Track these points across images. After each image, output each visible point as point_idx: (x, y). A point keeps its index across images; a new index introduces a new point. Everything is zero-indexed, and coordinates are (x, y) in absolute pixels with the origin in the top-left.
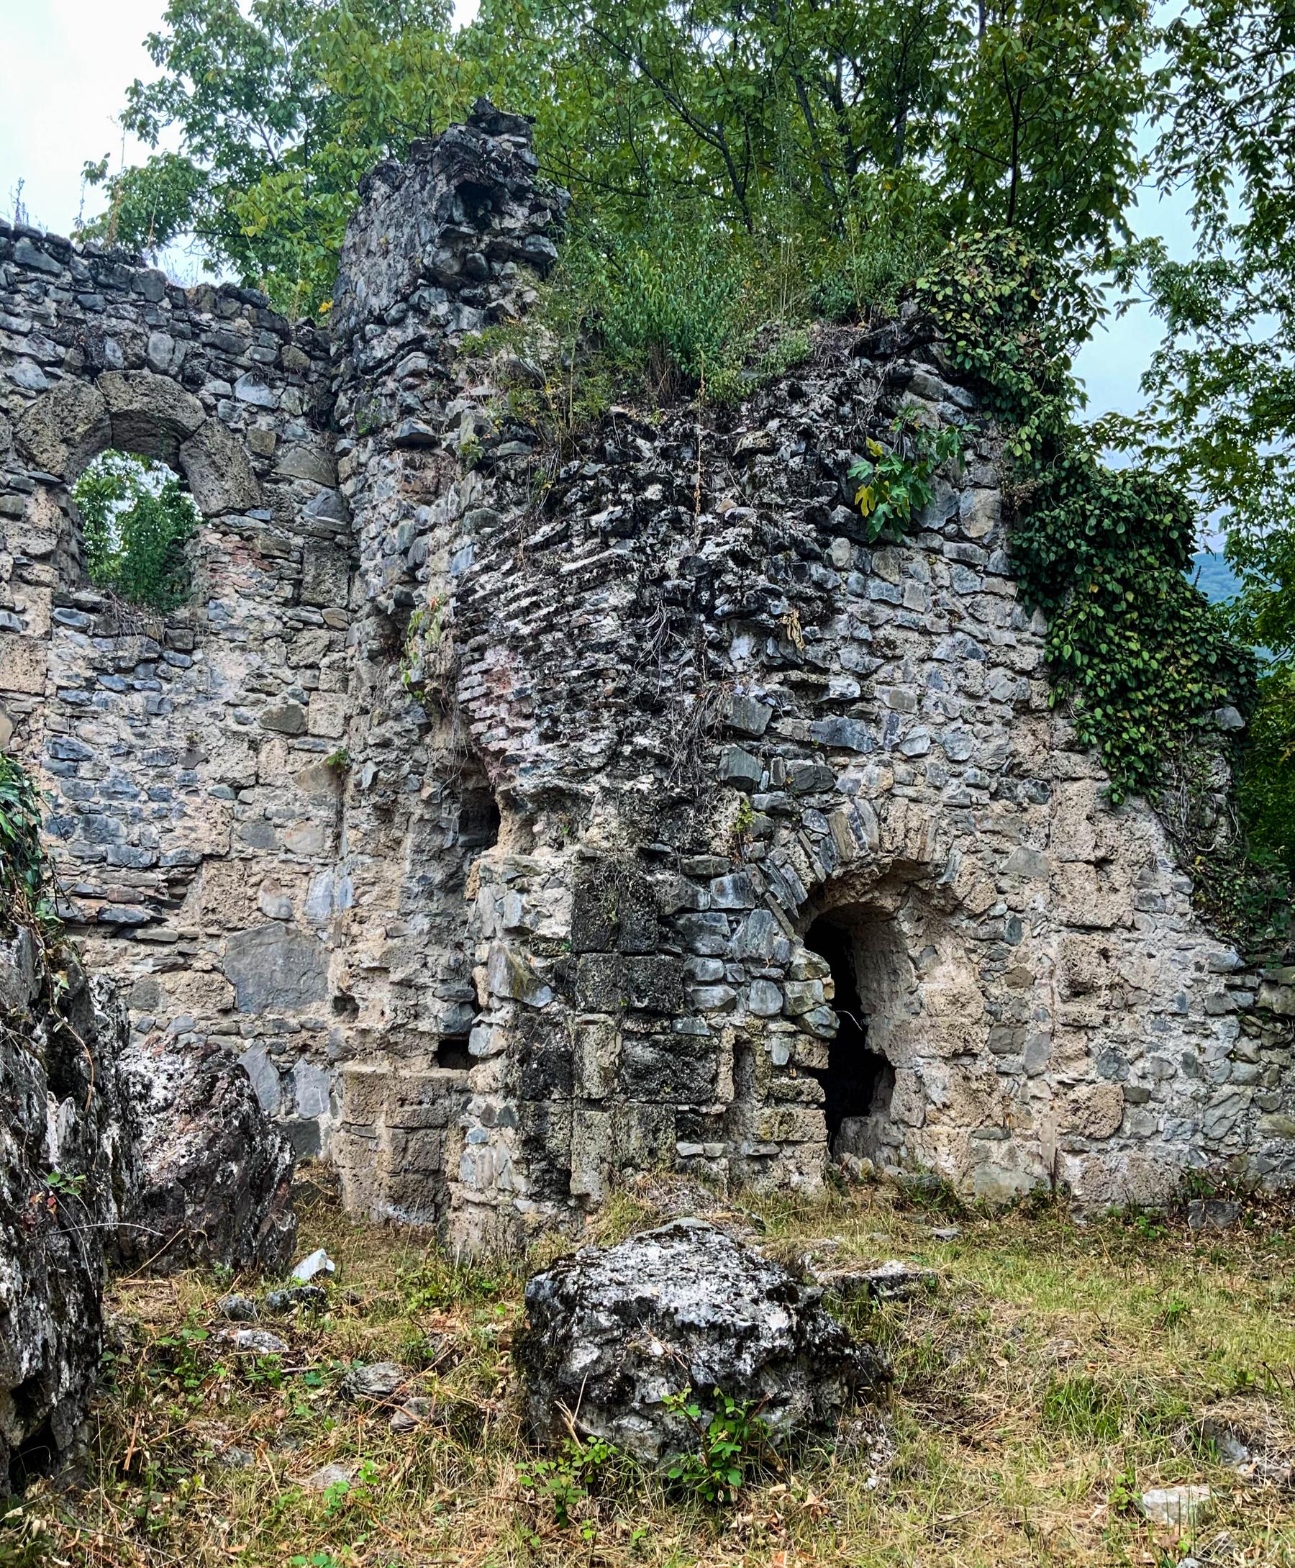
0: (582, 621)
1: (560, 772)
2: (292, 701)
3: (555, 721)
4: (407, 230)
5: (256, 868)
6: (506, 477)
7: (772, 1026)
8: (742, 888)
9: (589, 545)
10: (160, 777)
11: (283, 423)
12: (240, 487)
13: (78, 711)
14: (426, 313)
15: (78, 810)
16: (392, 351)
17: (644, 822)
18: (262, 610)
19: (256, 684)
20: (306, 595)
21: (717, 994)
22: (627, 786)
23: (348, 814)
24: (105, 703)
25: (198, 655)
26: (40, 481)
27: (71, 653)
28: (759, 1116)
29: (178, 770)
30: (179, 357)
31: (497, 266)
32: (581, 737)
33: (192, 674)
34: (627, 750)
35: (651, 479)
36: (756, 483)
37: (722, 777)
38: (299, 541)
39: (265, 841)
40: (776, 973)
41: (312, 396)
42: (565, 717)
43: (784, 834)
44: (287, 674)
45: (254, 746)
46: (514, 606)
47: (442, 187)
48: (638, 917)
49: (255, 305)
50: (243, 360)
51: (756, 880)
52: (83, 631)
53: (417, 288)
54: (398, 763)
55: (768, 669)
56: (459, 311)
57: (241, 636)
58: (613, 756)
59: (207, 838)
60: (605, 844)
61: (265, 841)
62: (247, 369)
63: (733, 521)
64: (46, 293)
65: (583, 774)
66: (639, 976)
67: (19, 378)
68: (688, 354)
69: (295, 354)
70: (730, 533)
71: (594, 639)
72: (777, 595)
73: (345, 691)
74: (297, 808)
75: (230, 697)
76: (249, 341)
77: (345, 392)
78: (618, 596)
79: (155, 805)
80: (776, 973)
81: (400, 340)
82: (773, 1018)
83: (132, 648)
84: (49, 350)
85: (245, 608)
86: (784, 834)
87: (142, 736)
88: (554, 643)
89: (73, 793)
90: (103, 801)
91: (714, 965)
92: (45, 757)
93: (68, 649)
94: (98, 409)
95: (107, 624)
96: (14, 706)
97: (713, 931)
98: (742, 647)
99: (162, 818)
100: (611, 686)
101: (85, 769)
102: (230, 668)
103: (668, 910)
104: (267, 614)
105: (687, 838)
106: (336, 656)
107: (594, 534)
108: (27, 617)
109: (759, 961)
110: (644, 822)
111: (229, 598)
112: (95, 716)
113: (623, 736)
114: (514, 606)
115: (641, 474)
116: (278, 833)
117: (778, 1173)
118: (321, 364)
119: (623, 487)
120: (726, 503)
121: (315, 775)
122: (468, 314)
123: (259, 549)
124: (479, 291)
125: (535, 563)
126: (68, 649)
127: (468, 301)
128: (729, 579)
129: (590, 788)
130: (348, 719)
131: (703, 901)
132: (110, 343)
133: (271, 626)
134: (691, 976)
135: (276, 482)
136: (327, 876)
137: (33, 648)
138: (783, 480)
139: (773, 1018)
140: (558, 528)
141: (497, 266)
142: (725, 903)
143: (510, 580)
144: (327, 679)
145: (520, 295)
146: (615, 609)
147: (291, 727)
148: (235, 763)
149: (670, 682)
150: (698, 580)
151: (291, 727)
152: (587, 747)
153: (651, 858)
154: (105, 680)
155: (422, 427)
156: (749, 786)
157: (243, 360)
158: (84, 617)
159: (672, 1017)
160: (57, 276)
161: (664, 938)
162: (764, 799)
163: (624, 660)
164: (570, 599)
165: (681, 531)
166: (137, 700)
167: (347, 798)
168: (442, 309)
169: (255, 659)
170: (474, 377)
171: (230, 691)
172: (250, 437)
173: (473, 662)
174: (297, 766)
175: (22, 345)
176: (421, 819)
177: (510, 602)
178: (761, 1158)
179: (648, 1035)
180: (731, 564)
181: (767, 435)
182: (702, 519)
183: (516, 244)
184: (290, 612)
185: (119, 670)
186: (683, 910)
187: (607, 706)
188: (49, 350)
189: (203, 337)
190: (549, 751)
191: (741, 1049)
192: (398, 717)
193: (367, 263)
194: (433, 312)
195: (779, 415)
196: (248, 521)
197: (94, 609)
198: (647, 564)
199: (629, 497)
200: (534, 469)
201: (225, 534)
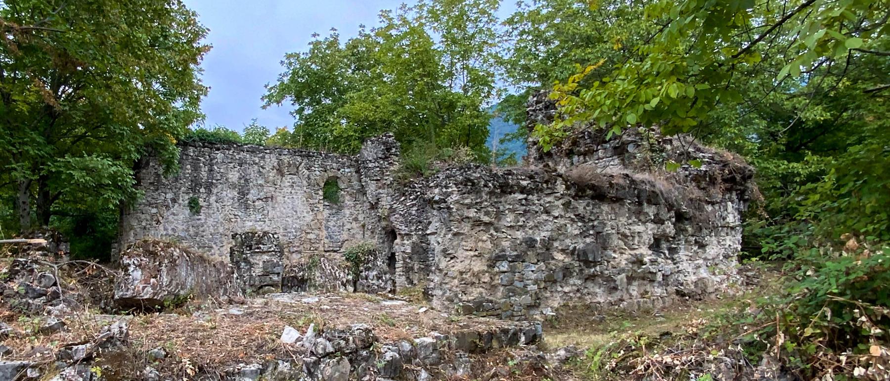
69: (353, 163)
83: (334, 211)
102: (347, 212)
104: (351, 203)
147: (356, 219)
151: (356, 219)
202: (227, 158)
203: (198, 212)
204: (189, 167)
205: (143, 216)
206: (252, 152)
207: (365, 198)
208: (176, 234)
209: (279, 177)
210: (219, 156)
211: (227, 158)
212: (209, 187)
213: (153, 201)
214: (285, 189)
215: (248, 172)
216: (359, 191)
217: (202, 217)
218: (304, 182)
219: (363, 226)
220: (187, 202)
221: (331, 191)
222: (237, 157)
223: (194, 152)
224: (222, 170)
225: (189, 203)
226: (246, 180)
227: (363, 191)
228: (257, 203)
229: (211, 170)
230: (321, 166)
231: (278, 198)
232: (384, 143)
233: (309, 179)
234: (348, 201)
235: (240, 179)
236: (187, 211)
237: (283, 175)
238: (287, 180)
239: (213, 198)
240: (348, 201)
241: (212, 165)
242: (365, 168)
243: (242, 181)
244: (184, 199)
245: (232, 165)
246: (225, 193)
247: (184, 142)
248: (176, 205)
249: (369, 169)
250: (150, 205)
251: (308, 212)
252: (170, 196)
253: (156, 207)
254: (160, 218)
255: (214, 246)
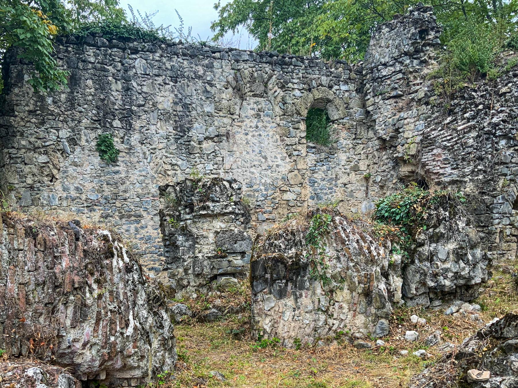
0: (465, 141)
1: (458, 176)
2: (356, 163)
3: (457, 165)
4: (397, 42)
5: (350, 202)
6: (434, 106)
7: (507, 227)
8: (503, 198)
9: (463, 122)
10: (330, 184)
11: (351, 94)
12: (343, 112)
13: (314, 172)
14: (403, 63)
15: (315, 194)
16: (390, 74)
17: (480, 186)
18: (349, 142)
19: (348, 160)
20: (358, 137)
21: (497, 221)
22: (476, 178)
23: (369, 188)
24: (319, 169)
25: (336, 155)
26: (302, 119)
27: (312, 158)
28: (504, 245)
29: (334, 182)
30: (328, 81)
31: (424, 48)
32: (465, 168)
33: (335, 160)
34: (476, 170)
35: (480, 104)
36: (506, 101)
37: (499, 174)
38: (355, 123)
39: (352, 196)
40: (509, 215)
41: (357, 85)
42: (461, 164)
43: (512, 185)
44: (354, 157)
45: (348, 175)
46: (443, 139)
47: (413, 30)
48: (482, 206)
49: (344, 64)
50: (342, 79)
51: (506, 196)
52: (313, 153)
53: (401, 57)
54: (387, 175)
55: (509, 147)
56: (412, 61)
57: (344, 149)
58: (473, 172)
59: (340, 197)
60: (470, 191)
61: (352, 196)
62: (342, 82)
63: (502, 111)
64: (299, 71)
65: (464, 176)
66: (482, 219)
67: (296, 95)
68: (482, 67)
69: (353, 75)
70: (501, 115)
71: (468, 145)
72: (513, 129)
73: (367, 159)
74: (358, 188)
75: (343, 164)
76: (343, 74)
77: (369, 84)
78: (474, 134)
79: (330, 191)
80: (509, 215)
81: (393, 70)
82: (507, 225)
83: (323, 155)
84: (302, 86)
85: (345, 142)
86: (512, 185)
87: (326, 175)
88: (458, 147)
89: (315, 190)
90: (320, 191)
91: (497, 215)
92: (308, 183)
93: (311, 158)
94: (312, 99)
95: (318, 151)
96: (302, 172)
97: (497, 208)
98: (503, 142)
99: (331, 193)
100: (473, 156)
101: (316, 185)
103: (488, 204)
104: (349, 143)
105: (491, 189)
106: (365, 151)
107: (465, 119)
108: (302, 152)
109: (506, 213)
110: (480, 186)
111: (342, 141)
112: (317, 172)
113: (476, 167)
114: (445, 139)
115: (477, 103)
116: (355, 194)
117: (506, 257)
118: (359, 76)
119: (472, 107)
120: (497, 106)
121: (361, 180)
122: (415, 62)
123: (347, 127)
124: (419, 56)
125: (448, 128)
126: (311, 158)
127: (415, 59)
128: (501, 126)
129: (466, 179)
130: (369, 166)
131: (495, 202)
132: (314, 81)
133: (351, 146)
134: (492, 217)
135: (349, 109)
136: (365, 203)
137: (304, 159)
138: (513, 99)
139: (507, 225)
140: (454, 118)
141: (424, 48)
142: (500, 202)
143: (442, 132)
144: (363, 156)
145: (429, 55)
146: (473, 137)
147: (356, 169)
148: (344, 179)
149: (484, 153)
150: (492, 127)
151: (356, 169)
152: (466, 170)
153: (483, 193)
154: (318, 164)
155: (400, 92)
156: (505, 175)
157: (342, 79)
158: (314, 150)
159: (488, 227)
160: (301, 66)
161: (487, 210)
162: (508, 177)
163: (474, 149)
164: (461, 136)
165: (486, 115)
166: (325, 167)
167: (370, 184)
168: (408, 61)
169: (348, 154)
170: (415, 78)
171: (343, 163)
172: (344, 99)
173: (429, 152)
174: (358, 178)
175: (296, 86)
176: (392, 187)
177: (443, 138)
178: (503, 254)
179: (482, 231)
180: (502, 123)
181: (509, 88)
182: (492, 112)
183: (431, 42)
184: (354, 142)
185: (321, 161)
186: (491, 204)
187: (472, 160)
188: (302, 86)
189: (332, 75)
190: (455, 172)
191: (501, 232)
192: (386, 164)
193: (379, 50)
194: (405, 63)
195: (512, 82)
196: (344, 121)
197: (314, 148)
198: (479, 125)
199: (474, 109)
200: (442, 103)
201: (338, 124)
202: (152, 66)
203: (114, 161)
204: (90, 82)
205: (27, 169)
206: (192, 56)
207: (371, 134)
208: (84, 197)
209: (238, 100)
210: (139, 63)
211: (152, 66)
212: (127, 117)
213: (39, 143)
214: (247, 121)
215: (188, 91)
216: (361, 123)
217: (121, 167)
218: (277, 109)
219: (367, 179)
220: (94, 143)
221: (317, 121)
222: (168, 66)
223: (96, 55)
224: (145, 89)
225: (98, 145)
226: (186, 106)
227: (368, 120)
228: (205, 145)
229: (127, 89)
230: (304, 80)
231: (238, 136)
232: (415, 22)
233: (284, 103)
234: (344, 139)
235: (175, 103)
236: (96, 160)
237: (242, 98)
238: (251, 105)
239: (135, 138)
240: (344, 139)
241: (127, 80)
242: (374, 80)
243: (179, 108)
244: (89, 138)
245: (160, 80)
246: (153, 128)
247: (78, 37)
248: (78, 149)
249: (381, 80)
250: (35, 149)
251: (283, 159)
252: (64, 133)
253: (46, 153)
254: (55, 172)
255: (144, 214)
